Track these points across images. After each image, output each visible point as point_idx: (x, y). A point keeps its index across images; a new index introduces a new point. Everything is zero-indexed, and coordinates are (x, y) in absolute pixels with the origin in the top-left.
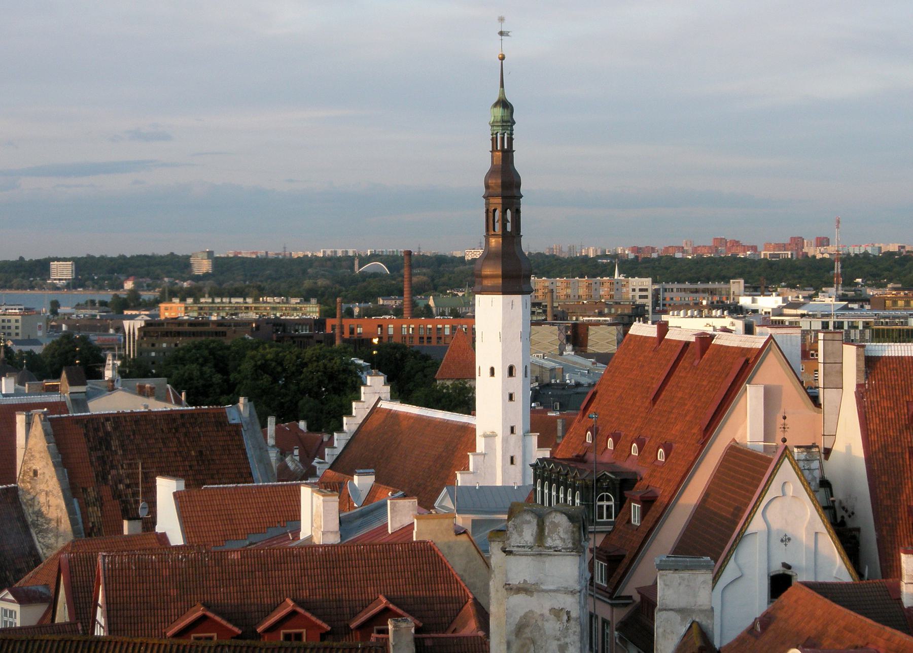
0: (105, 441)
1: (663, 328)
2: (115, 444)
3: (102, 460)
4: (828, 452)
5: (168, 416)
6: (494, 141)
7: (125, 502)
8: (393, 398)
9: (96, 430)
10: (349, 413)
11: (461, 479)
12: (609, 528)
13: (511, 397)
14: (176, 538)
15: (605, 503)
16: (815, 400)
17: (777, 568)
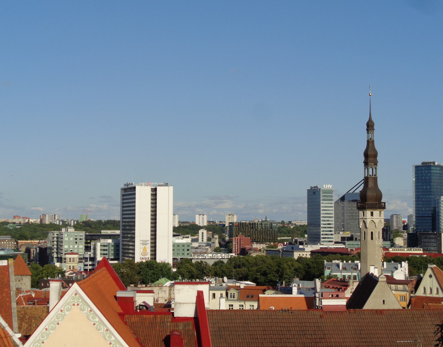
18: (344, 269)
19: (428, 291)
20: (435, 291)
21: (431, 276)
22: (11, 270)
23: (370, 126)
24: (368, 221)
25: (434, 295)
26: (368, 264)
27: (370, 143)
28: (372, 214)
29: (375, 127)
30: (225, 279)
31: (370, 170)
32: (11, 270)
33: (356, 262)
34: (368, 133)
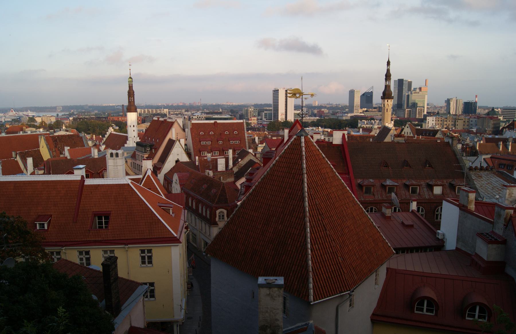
0: (56, 140)
1: (158, 118)
2: (58, 141)
3: (55, 144)
4: (186, 139)
5: (68, 135)
6: (129, 85)
7: (60, 151)
8: (114, 131)
9: (54, 138)
10: (106, 134)
11: (126, 145)
12: (149, 153)
13: (134, 131)
14: (69, 158)
15: (148, 149)
16: (184, 130)
17: (176, 159)
18: (367, 124)
19: (406, 133)
20: (409, 134)
21: (408, 127)
22: (245, 124)
23: (388, 63)
24: (386, 104)
25: (409, 135)
26: (385, 122)
27: (388, 71)
28: (388, 101)
29: (390, 64)
30: (320, 128)
31: (388, 82)
32: (245, 124)
33: (372, 121)
34: (387, 66)
